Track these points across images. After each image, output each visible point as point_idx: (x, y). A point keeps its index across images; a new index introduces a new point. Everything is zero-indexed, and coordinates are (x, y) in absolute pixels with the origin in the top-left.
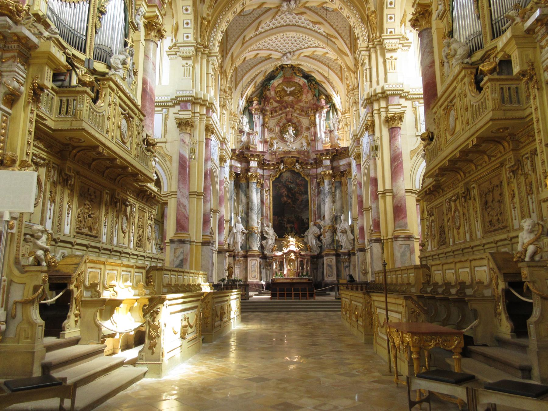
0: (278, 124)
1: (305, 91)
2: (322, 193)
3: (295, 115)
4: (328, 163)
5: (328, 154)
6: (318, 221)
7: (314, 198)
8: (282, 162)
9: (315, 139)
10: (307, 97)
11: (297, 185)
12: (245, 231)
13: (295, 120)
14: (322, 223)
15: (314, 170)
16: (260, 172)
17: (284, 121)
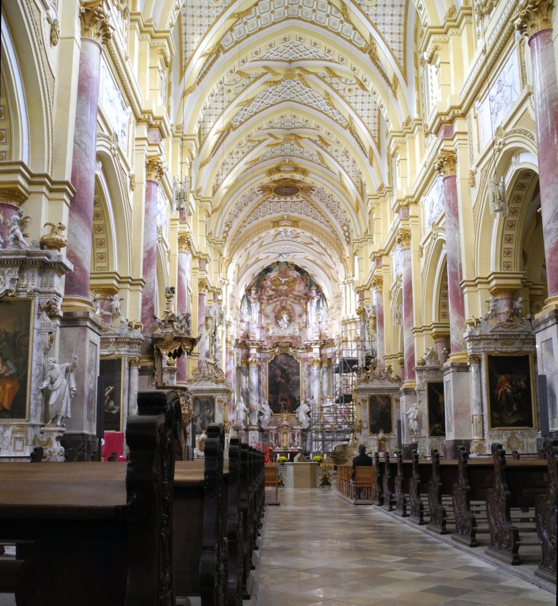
0: (274, 311)
2: (312, 375)
6: (308, 400)
7: (305, 379)
9: (306, 324)
10: (300, 288)
13: (289, 307)
15: (306, 354)
17: (279, 307)
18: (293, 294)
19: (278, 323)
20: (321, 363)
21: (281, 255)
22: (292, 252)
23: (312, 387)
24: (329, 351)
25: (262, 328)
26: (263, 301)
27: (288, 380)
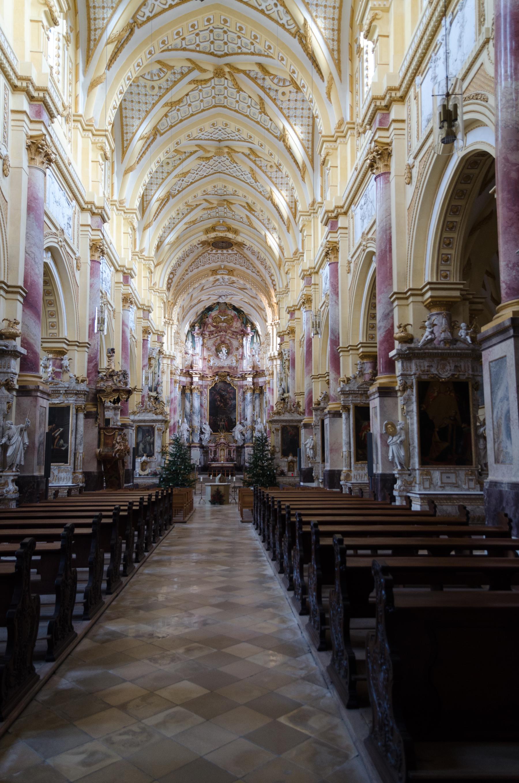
0: (214, 345)
3: (228, 337)
4: (250, 379)
5: (249, 374)
6: (242, 421)
8: (217, 375)
9: (242, 357)
10: (237, 325)
13: (228, 342)
16: (200, 383)
17: (219, 342)
20: (254, 391)
21: (220, 297)
24: (261, 380)
27: (226, 404)
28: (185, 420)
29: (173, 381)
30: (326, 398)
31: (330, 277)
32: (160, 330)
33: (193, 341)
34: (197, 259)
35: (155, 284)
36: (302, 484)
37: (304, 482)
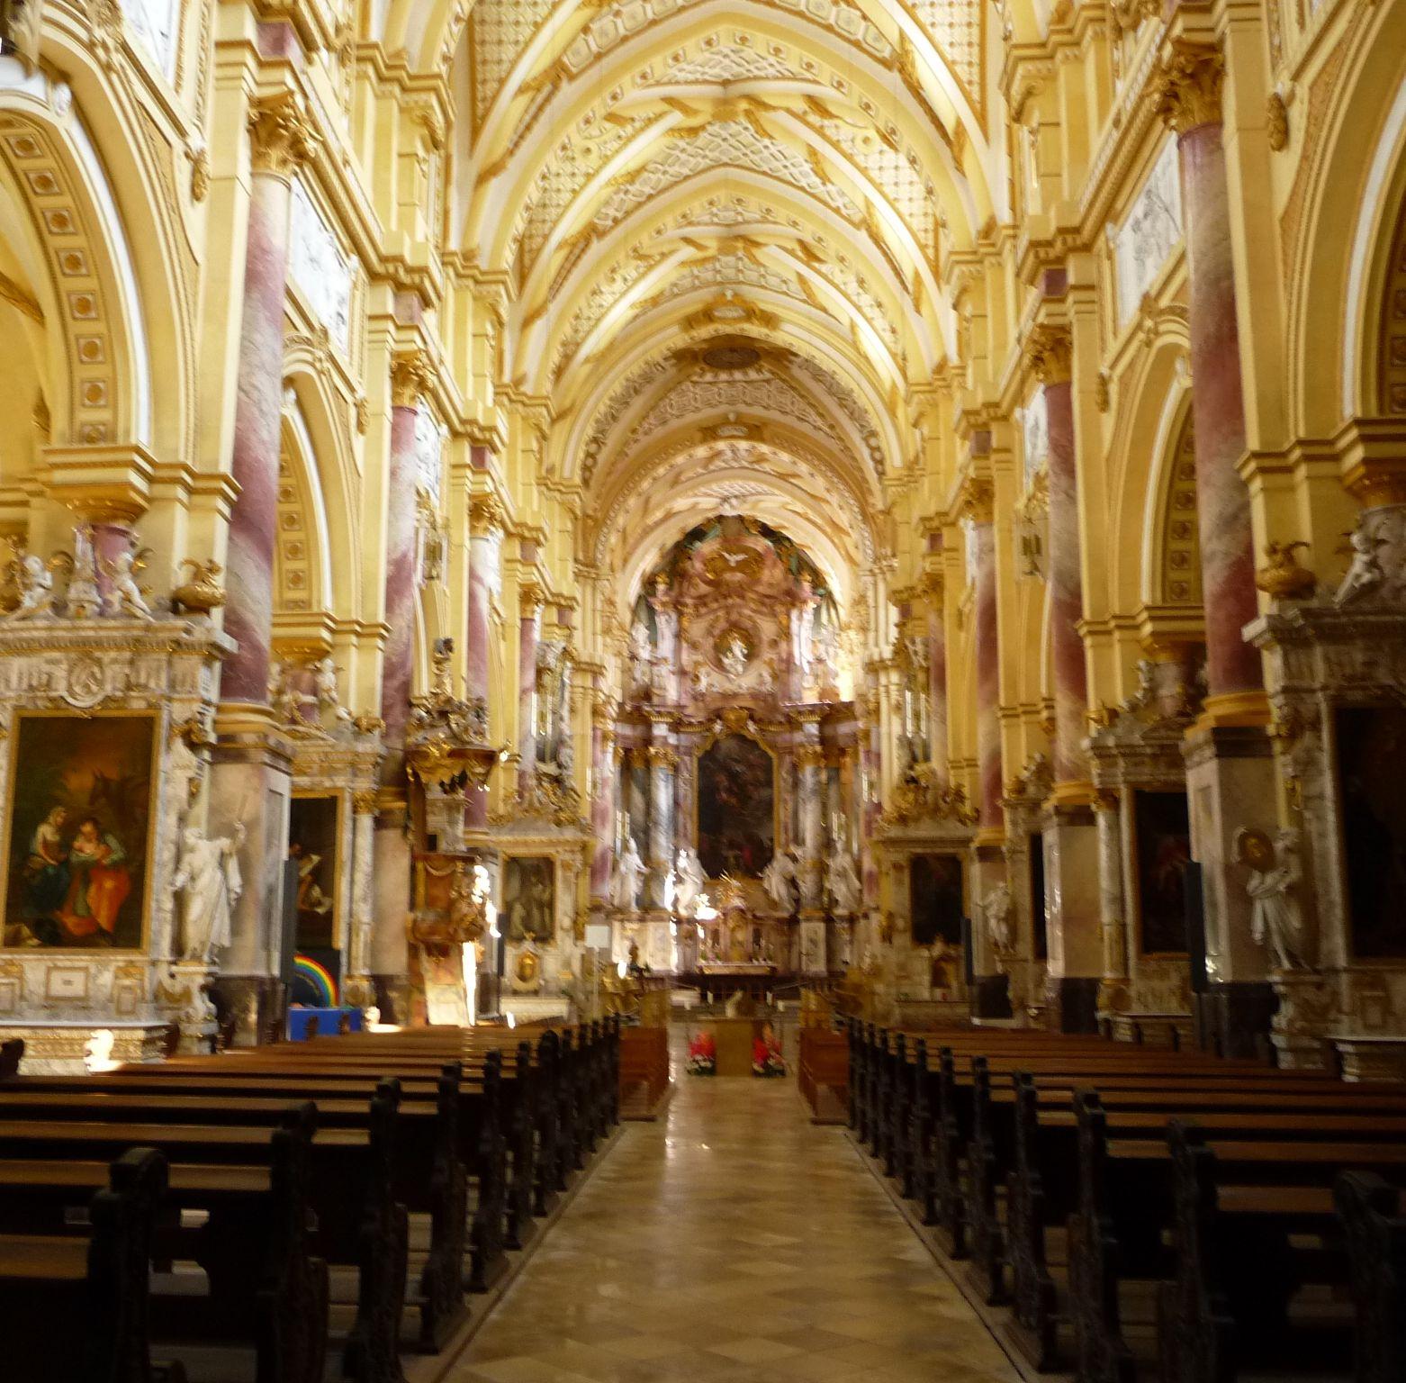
0: (709, 633)
1: (769, 562)
4: (812, 729)
5: (812, 712)
6: (793, 849)
8: (719, 717)
10: (773, 574)
11: (751, 766)
12: (645, 870)
13: (748, 624)
14: (798, 852)
15: (787, 736)
16: (672, 740)
17: (722, 624)
18: (757, 592)
19: (720, 661)
22: (752, 494)
23: (801, 815)
24: (844, 729)
25: (682, 673)
26: (686, 610)
27: (744, 797)
28: (633, 844)
29: (599, 733)
30: (1045, 772)
31: (1050, 425)
32: (566, 593)
33: (652, 626)
34: (661, 399)
35: (551, 470)
36: (976, 1021)
37: (983, 1015)
